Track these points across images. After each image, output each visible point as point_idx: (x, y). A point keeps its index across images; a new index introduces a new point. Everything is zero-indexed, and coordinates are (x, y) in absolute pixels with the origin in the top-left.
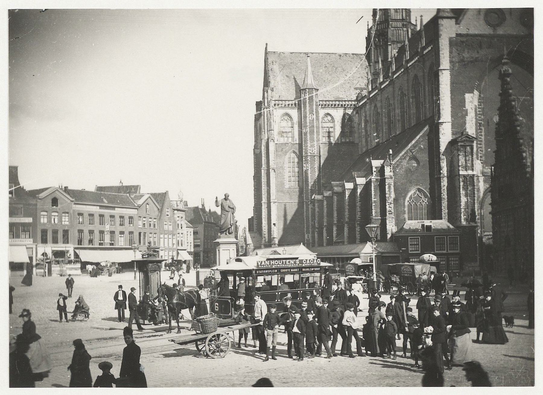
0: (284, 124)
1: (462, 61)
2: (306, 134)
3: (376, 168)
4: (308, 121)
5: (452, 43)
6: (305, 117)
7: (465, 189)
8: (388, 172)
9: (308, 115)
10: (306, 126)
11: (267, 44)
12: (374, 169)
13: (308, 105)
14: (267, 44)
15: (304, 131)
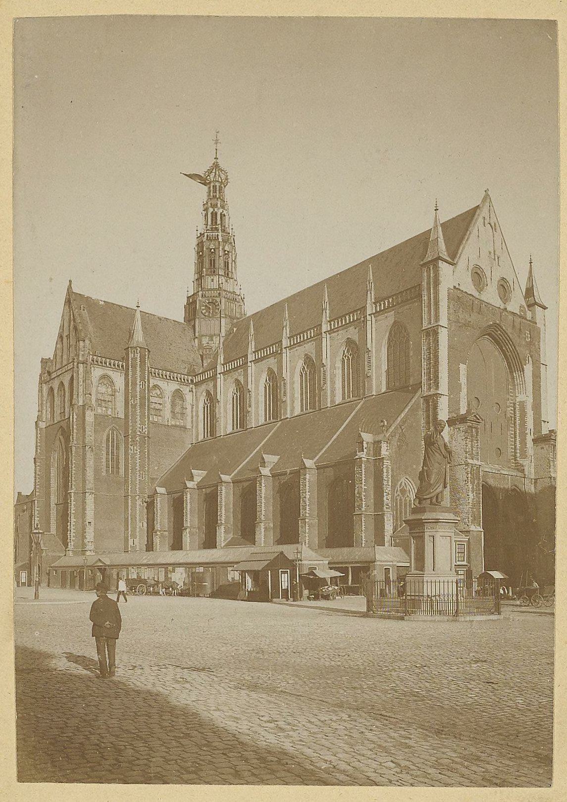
0: (103, 389)
1: (458, 321)
2: (134, 406)
3: (367, 443)
4: (138, 390)
5: (450, 297)
6: (134, 384)
7: (473, 483)
8: (385, 451)
9: (138, 382)
10: (134, 397)
11: (70, 281)
12: (365, 445)
13: (138, 369)
14: (70, 281)
15: (131, 402)
